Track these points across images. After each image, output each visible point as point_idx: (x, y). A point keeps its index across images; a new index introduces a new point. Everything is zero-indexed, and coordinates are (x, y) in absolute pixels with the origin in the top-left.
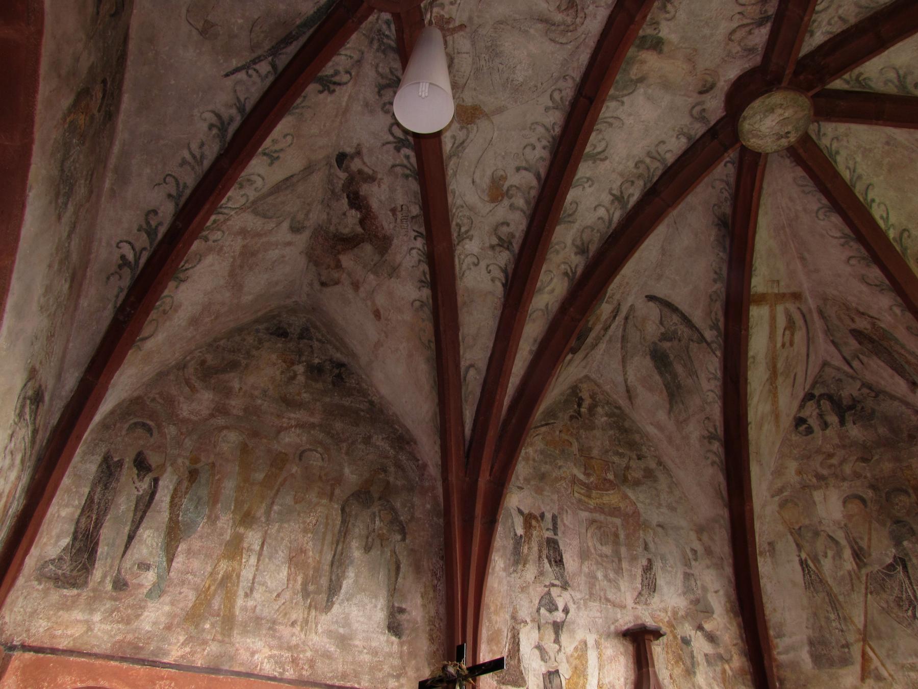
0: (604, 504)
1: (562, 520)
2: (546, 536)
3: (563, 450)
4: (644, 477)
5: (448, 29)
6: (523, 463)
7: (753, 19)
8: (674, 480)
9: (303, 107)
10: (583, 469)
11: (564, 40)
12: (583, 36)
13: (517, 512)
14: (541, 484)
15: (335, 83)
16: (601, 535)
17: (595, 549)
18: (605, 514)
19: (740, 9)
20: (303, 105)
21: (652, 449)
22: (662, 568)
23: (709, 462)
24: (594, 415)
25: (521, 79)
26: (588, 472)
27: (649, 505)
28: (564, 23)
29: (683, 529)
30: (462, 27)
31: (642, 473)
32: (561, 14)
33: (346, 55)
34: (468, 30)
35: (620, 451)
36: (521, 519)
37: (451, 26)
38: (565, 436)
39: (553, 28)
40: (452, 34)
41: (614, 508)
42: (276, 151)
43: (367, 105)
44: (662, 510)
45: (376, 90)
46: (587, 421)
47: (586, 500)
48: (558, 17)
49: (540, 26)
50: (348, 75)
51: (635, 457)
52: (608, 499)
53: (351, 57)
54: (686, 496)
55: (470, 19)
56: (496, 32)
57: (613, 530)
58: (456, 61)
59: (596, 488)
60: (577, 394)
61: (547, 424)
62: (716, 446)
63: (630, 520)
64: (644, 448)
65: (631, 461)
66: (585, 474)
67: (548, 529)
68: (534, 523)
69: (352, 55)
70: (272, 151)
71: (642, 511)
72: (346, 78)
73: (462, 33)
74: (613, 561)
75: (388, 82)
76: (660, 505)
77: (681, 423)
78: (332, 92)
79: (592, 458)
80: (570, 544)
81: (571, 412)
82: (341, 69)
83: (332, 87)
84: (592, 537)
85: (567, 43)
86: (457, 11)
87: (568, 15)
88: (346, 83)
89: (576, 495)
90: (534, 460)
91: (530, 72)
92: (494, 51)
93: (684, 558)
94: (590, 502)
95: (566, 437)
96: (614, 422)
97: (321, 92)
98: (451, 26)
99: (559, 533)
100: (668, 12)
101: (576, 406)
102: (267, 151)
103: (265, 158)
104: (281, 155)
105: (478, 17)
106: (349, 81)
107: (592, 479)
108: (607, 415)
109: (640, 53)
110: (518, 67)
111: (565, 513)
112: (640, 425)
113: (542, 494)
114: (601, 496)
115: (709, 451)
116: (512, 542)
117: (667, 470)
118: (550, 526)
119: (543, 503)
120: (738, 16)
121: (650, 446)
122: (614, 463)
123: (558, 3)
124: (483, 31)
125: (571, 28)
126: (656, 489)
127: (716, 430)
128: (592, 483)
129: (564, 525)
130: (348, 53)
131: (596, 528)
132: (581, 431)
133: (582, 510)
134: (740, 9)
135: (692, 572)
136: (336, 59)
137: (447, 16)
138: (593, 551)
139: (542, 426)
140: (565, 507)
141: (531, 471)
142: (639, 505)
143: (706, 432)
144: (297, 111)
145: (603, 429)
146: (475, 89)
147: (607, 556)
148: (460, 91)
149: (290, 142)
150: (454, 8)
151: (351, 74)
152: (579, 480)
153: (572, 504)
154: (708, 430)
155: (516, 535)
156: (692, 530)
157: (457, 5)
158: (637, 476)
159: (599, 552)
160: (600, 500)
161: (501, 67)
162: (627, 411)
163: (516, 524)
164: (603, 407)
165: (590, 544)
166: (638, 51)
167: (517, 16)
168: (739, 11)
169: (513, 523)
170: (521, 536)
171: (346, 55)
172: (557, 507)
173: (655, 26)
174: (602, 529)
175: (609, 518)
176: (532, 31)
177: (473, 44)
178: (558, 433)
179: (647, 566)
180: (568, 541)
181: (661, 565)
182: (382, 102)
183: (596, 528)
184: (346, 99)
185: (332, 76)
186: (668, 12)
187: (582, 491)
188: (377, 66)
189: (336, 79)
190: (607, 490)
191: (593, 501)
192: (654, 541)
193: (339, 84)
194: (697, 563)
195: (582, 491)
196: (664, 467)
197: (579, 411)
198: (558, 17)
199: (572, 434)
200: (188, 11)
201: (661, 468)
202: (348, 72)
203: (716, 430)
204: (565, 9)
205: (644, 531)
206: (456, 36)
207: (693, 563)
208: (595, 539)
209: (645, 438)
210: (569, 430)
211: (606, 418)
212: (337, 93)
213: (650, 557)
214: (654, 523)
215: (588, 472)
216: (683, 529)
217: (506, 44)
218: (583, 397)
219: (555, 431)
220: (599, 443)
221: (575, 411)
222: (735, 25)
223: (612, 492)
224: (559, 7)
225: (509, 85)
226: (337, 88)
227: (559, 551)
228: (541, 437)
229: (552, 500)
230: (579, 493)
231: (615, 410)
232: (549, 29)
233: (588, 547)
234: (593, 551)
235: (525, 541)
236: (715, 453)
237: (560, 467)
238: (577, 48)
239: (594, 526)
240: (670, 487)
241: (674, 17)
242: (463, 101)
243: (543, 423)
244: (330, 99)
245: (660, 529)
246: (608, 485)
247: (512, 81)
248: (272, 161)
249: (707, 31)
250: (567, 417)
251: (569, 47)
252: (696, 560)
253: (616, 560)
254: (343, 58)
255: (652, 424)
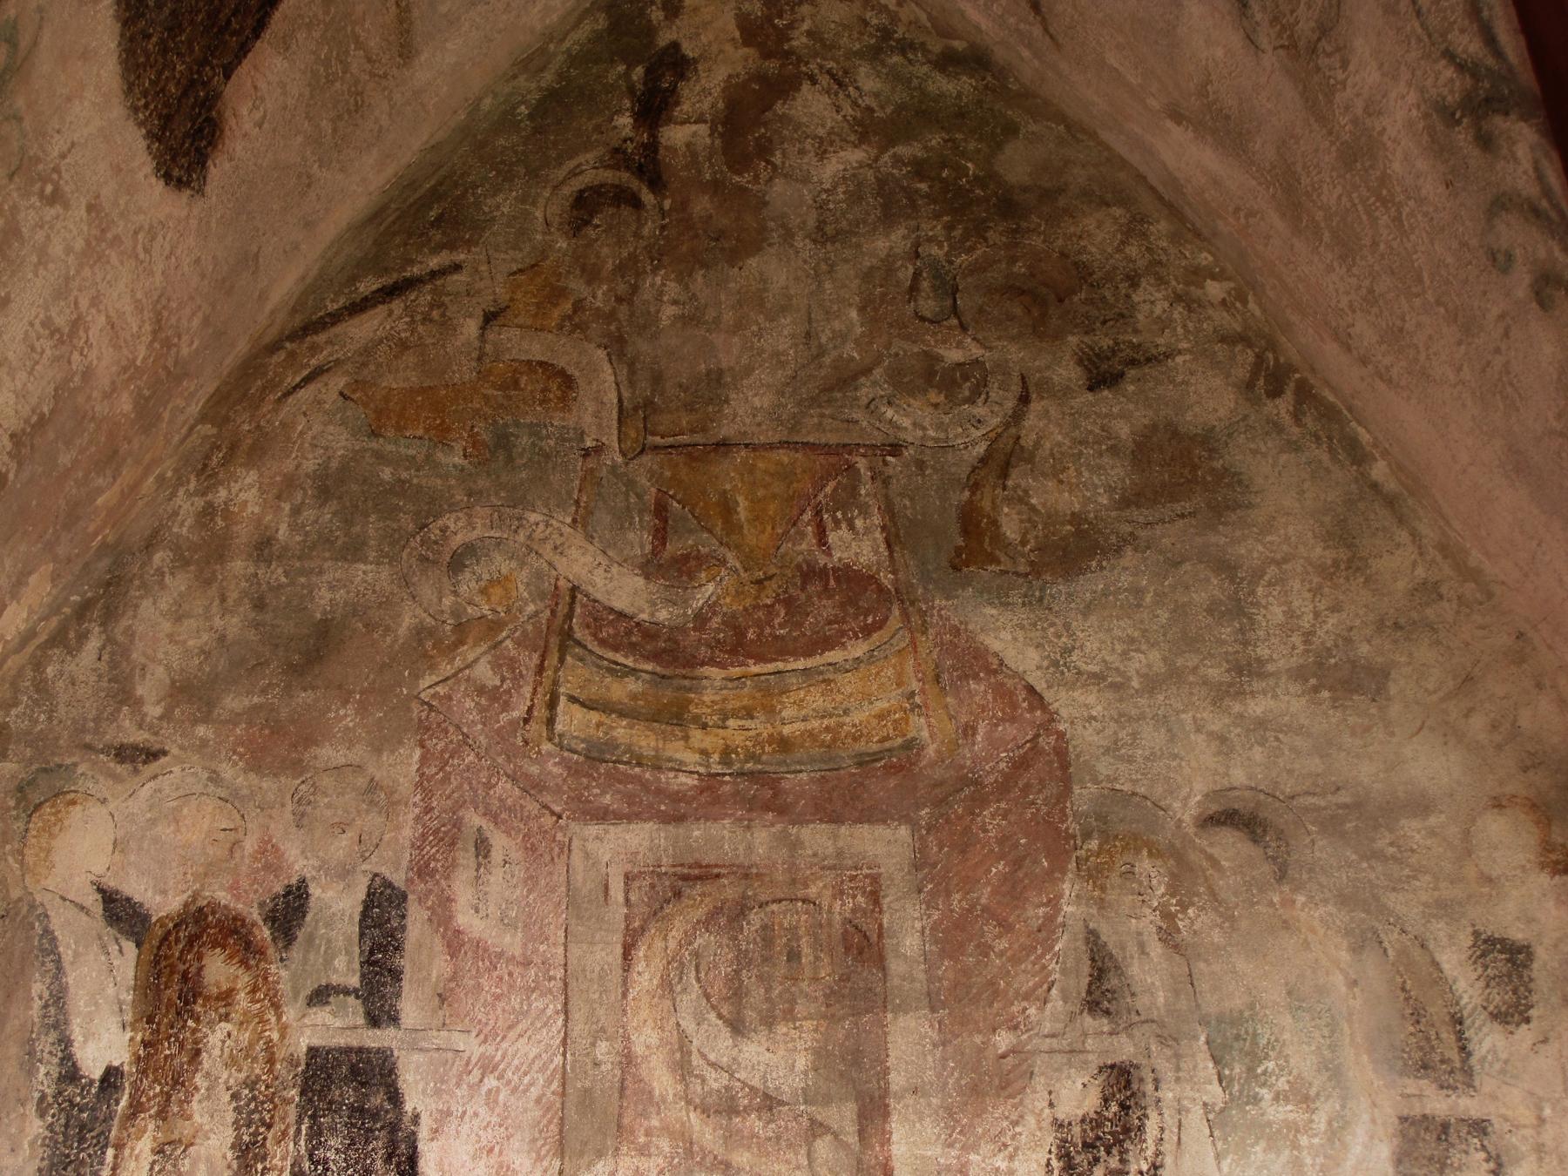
0: (784, 744)
1: (442, 916)
2: (302, 1043)
3: (503, 441)
4: (1125, 503)
6: (178, 583)
8: (1379, 470)
10: (639, 540)
13: (97, 922)
14: (304, 697)
16: (742, 960)
17: (682, 1068)
18: (782, 811)
21: (1214, 290)
22: (1217, 1120)
23: (1521, 282)
24: (764, 150)
26: (673, 548)
27: (1152, 684)
29: (1421, 806)
31: (1118, 472)
35: (953, 355)
36: (126, 959)
38: (521, 345)
41: (863, 761)
44: (1257, 707)
46: (702, 205)
47: (645, 740)
51: (1067, 372)
52: (816, 699)
54: (1474, 575)
57: (841, 909)
59: (737, 646)
60: (650, 31)
61: (389, 293)
62: (1522, 151)
63: (991, 821)
64: (1151, 301)
65: (1036, 406)
66: (650, 568)
67: (320, 996)
68: (218, 969)
71: (1086, 739)
74: (816, 1129)
76: (1246, 670)
77: (1313, 50)
79: (723, 446)
80: (488, 1067)
81: (589, 169)
84: (667, 986)
89: (571, 720)
90: (263, 548)
93: (1417, 1016)
94: (676, 750)
95: (536, 349)
96: (919, 169)
99: (411, 1008)
101: (625, 121)
107: (706, 592)
108: (865, 129)
111: (466, 858)
112: (1121, 147)
113: (297, 767)
114: (768, 697)
115: (1500, 204)
116: (36, 1127)
117: (1329, 414)
118: (346, 970)
119: (300, 820)
121: (1197, 275)
122: (895, 449)
126: (1226, 567)
127: (1490, 40)
128: (701, 619)
129: (455, 943)
131: (707, 923)
132: (652, 282)
133: (602, 816)
135: (1468, 1105)
138: (662, 1081)
139: (359, 307)
140: (474, 819)
141: (233, 625)
142: (1068, 704)
143: (1450, 73)
145: (821, 236)
147: (769, 1103)
152: (606, 619)
153: (533, 787)
154: (1449, 55)
155: (70, 1074)
156: (1498, 804)
158: (1068, 502)
159: (716, 1081)
160: (759, 726)
162: (1025, 63)
163: (79, 1002)
164: (840, 81)
165: (646, 1039)
169: (58, 998)
170: (111, 1078)
172: (408, 832)
174: (756, 918)
175: (816, 838)
178: (471, 328)
179: (1097, 1122)
180: (471, 1046)
181: (1214, 1092)
183: (707, 923)
187: (621, 690)
190: (827, 644)
191: (696, 735)
192: (1168, 935)
194: (1525, 1035)
195: (621, 690)
196: (1305, 393)
197: (652, 147)
199: (575, 323)
201: (1282, 407)
203: (1490, 40)
205: (1094, 875)
207: (1488, 1041)
208: (690, 998)
209: (1161, 227)
210: (558, 294)
211: (855, 156)
213: (1124, 1049)
214: (1186, 808)
215: (673, 548)
216: (1421, 806)
218: (689, 50)
219: (447, 326)
220: (782, 336)
221: (618, 157)
223: (859, 649)
227: (394, 1128)
228: (339, 382)
229: (373, 786)
230: (588, 705)
231: (942, 85)
233: (628, 1060)
234: (662, 1081)
235: (136, 1108)
236: (1536, 212)
237: (457, 564)
239: (698, 902)
240: (1341, 534)
243: (368, 285)
245: (1229, 846)
246: (827, 608)
250: (549, 206)
252: (1512, 1014)
253: (843, 1116)
255: (1177, 117)
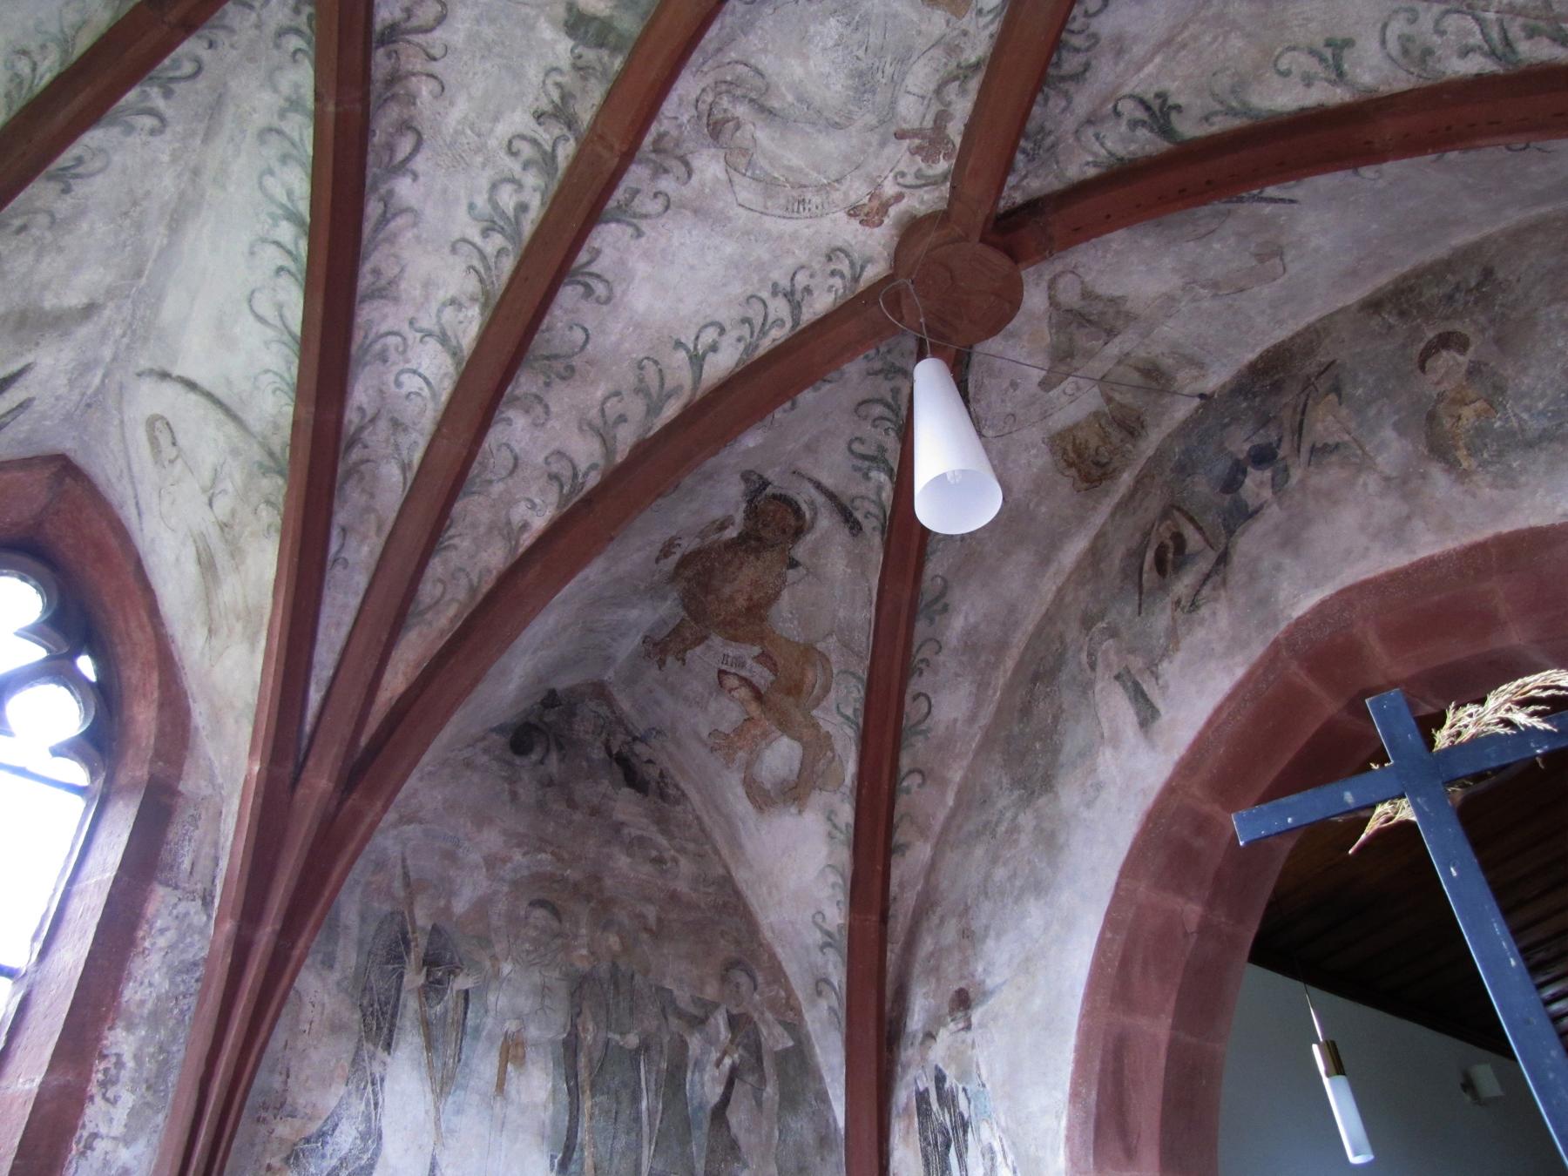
5: (923, 138)
7: (409, 42)
9: (1221, 103)
11: (740, 68)
12: (705, 69)
15: (1148, 108)
19: (435, 67)
20: (1218, 107)
25: (833, 22)
28: (735, 99)
30: (900, 136)
32: (736, 115)
33: (1102, 145)
34: (893, 129)
37: (917, 141)
39: (753, 95)
40: (921, 129)
42: (1322, 59)
43: (1119, 53)
45: (1088, 74)
48: (741, 110)
49: (775, 103)
50: (1119, 107)
53: (1097, 137)
55: (883, 144)
56: (850, 112)
58: (932, 87)
69: (1093, 139)
70: (1327, 67)
72: (1127, 107)
73: (905, 126)
75: (1062, 85)
78: (1162, 96)
82: (1123, 128)
83: (1156, 105)
85: (737, 62)
86: (898, 162)
87: (725, 111)
88: (1131, 96)
91: (812, 29)
92: (863, 83)
97: (1178, 108)
98: (917, 141)
100: (558, 85)
102: (1333, 76)
103: (1346, 66)
104: (1319, 42)
105: (870, 144)
106: (1124, 97)
109: (607, 12)
110: (830, 43)
120: (437, 52)
123: (738, 134)
124: (871, 119)
125: (724, 87)
130: (1096, 147)
134: (435, 67)
136: (1121, 151)
137: (918, 158)
144: (1234, 104)
146: (919, 33)
148: (947, 39)
149: (1289, 55)
150: (902, 167)
151: (1115, 107)
157: (896, 170)
161: (861, 53)
166: (611, 17)
167: (808, 129)
168: (434, 63)
171: (1102, 145)
173: (580, 63)
176: (790, 98)
177: (893, 103)
182: (1089, 53)
184: (1150, 69)
185: (1144, 123)
186: (558, 85)
188: (1064, 110)
189: (1140, 114)
193: (1142, 102)
198: (741, 110)
200: (1274, 279)
202: (1117, 114)
204: (728, 121)
206: (916, 125)
212: (1156, 89)
217: (839, 87)
222: (438, 33)
224: (738, 127)
225: (857, 18)
226: (1149, 96)
232: (761, 95)
238: (719, 50)
241: (547, 74)
242: (948, 22)
244: (1171, 86)
247: (848, 24)
248: (1342, 48)
249: (488, 32)
251: (733, 55)
254: (1109, 144)
